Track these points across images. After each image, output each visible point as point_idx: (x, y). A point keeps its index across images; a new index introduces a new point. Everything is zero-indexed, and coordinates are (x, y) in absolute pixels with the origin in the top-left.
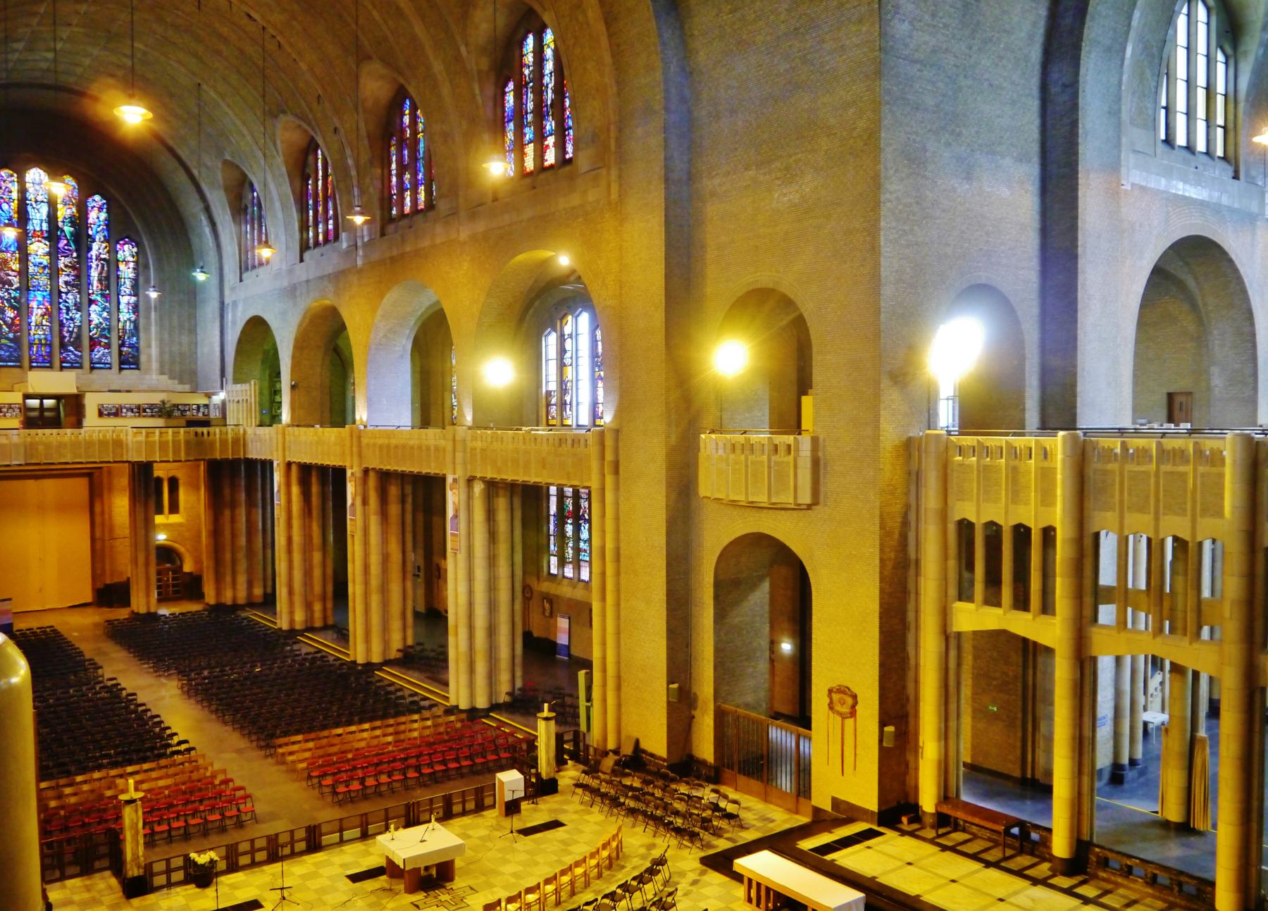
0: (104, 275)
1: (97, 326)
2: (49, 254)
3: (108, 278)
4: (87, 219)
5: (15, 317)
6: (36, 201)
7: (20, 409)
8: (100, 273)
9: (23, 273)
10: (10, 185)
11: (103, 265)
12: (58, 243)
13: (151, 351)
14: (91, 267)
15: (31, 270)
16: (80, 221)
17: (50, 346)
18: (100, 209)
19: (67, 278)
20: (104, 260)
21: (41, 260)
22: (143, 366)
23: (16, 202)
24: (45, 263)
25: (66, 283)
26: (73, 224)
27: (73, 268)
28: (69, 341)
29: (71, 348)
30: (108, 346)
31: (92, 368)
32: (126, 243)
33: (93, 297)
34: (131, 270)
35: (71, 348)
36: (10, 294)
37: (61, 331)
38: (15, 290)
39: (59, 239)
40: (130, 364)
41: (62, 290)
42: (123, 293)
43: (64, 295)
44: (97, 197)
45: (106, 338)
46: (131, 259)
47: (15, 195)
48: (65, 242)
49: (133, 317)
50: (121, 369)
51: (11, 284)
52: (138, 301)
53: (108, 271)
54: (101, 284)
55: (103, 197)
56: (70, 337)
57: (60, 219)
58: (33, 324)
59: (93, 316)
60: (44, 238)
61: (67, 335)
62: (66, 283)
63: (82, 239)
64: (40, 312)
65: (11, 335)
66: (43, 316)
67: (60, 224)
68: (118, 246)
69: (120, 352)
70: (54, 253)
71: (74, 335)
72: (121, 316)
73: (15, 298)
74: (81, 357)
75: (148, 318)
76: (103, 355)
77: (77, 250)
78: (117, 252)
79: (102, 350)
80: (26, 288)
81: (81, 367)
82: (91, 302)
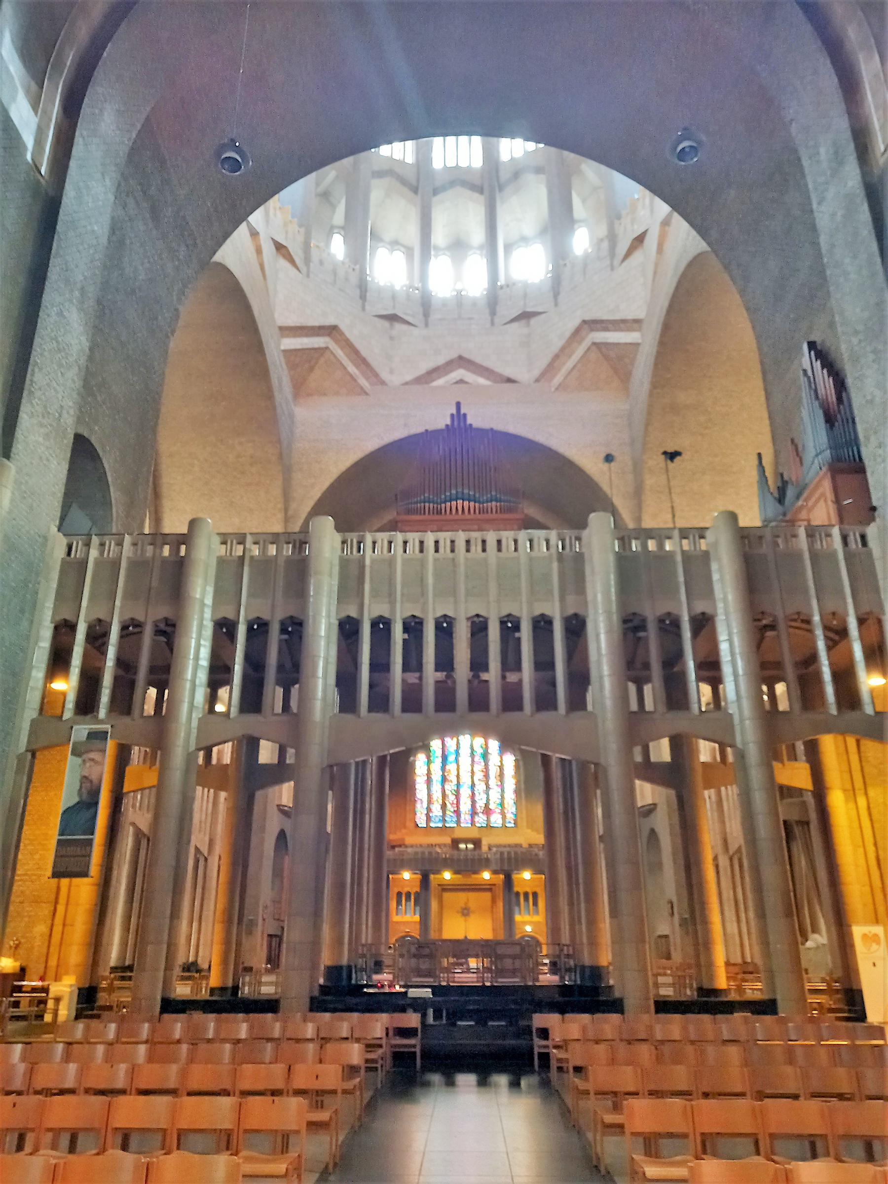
9: (458, 776)
71: (483, 808)
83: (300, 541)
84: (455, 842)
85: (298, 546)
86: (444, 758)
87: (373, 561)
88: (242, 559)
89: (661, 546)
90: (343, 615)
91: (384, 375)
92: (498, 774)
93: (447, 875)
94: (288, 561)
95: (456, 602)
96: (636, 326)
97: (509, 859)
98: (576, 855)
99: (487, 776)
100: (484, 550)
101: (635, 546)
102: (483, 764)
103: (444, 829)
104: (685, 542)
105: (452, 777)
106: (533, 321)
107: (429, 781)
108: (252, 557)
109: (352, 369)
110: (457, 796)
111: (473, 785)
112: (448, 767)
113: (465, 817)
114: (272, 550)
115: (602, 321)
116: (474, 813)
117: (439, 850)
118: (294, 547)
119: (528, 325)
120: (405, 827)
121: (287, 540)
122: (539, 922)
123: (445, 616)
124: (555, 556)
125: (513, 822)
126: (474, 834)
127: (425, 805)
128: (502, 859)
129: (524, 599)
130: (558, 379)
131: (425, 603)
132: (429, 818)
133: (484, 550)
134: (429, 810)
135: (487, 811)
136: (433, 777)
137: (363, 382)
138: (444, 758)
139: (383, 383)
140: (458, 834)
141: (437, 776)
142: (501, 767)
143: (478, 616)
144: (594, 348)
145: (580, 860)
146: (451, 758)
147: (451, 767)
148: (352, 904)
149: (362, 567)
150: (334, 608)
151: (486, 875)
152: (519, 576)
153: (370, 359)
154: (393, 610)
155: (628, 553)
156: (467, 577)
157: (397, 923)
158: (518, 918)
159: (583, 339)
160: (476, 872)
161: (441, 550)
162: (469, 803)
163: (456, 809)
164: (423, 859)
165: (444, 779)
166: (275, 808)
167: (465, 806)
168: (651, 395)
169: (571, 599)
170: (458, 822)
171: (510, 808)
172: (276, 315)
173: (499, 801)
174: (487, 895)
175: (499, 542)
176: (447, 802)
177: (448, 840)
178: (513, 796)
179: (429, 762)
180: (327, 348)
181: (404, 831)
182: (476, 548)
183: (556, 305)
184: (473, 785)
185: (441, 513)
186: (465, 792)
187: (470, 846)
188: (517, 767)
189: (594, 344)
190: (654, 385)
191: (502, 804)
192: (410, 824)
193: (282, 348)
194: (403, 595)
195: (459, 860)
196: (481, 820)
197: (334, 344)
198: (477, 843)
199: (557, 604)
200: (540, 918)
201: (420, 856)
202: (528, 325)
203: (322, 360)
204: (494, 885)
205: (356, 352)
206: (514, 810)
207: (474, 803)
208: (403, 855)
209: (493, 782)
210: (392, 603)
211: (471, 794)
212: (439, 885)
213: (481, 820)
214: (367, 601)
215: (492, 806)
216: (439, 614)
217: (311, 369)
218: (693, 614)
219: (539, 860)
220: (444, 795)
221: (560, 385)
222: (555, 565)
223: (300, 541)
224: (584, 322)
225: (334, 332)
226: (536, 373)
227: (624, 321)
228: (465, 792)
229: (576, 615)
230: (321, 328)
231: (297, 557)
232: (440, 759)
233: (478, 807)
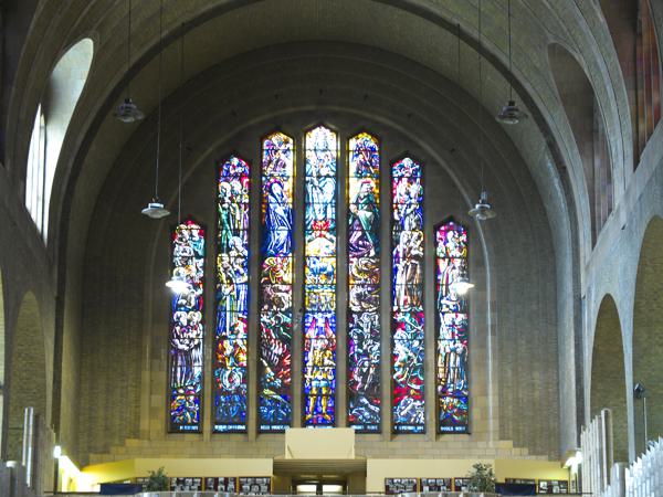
0: (416, 281)
1: (405, 364)
2: (335, 254)
3: (421, 286)
4: (393, 195)
5: (285, 354)
6: (319, 177)
7: (268, 485)
8: (412, 279)
9: (299, 286)
10: (283, 157)
11: (414, 266)
12: (349, 237)
13: (488, 403)
14: (396, 269)
15: (308, 281)
16: (382, 203)
17: (333, 397)
18: (411, 180)
19: (360, 290)
21: (325, 265)
22: (475, 428)
23: (291, 180)
24: (330, 269)
25: (359, 297)
26: (371, 205)
27: (371, 273)
28: (361, 389)
29: (365, 400)
30: (420, 396)
31: (395, 433)
32: (451, 229)
33: (400, 317)
34: (457, 271)
35: (365, 400)
36: (279, 319)
37: (349, 375)
38: (286, 313)
39: (350, 231)
40: (455, 423)
41: (354, 309)
42: (445, 309)
44: (407, 162)
45: (418, 382)
46: (458, 254)
47: (289, 171)
48: (360, 234)
49: (460, 347)
50: (439, 433)
51: (280, 304)
52: (467, 321)
53: (423, 274)
54: (411, 296)
55: (415, 160)
56: (364, 382)
57: (353, 199)
58: (310, 364)
59: (400, 349)
60: (328, 230)
61: (359, 379)
62: (359, 297)
63: (384, 227)
64: (320, 344)
65: (278, 382)
66: (324, 350)
67: (353, 208)
68: (438, 235)
69: (439, 408)
70: (345, 251)
71: (369, 380)
72: (441, 345)
73: (285, 325)
74: (380, 413)
75: (483, 346)
76: (413, 410)
77: (376, 245)
78: (436, 244)
79: (412, 403)
81: (378, 432)
82: (395, 326)
86: (260, 231)
120: (136, 434)
138: (260, 231)
141: (235, 292)
165: (259, 298)
177: (263, 467)
179: (215, 247)
181: (133, 443)
220: (258, 342)
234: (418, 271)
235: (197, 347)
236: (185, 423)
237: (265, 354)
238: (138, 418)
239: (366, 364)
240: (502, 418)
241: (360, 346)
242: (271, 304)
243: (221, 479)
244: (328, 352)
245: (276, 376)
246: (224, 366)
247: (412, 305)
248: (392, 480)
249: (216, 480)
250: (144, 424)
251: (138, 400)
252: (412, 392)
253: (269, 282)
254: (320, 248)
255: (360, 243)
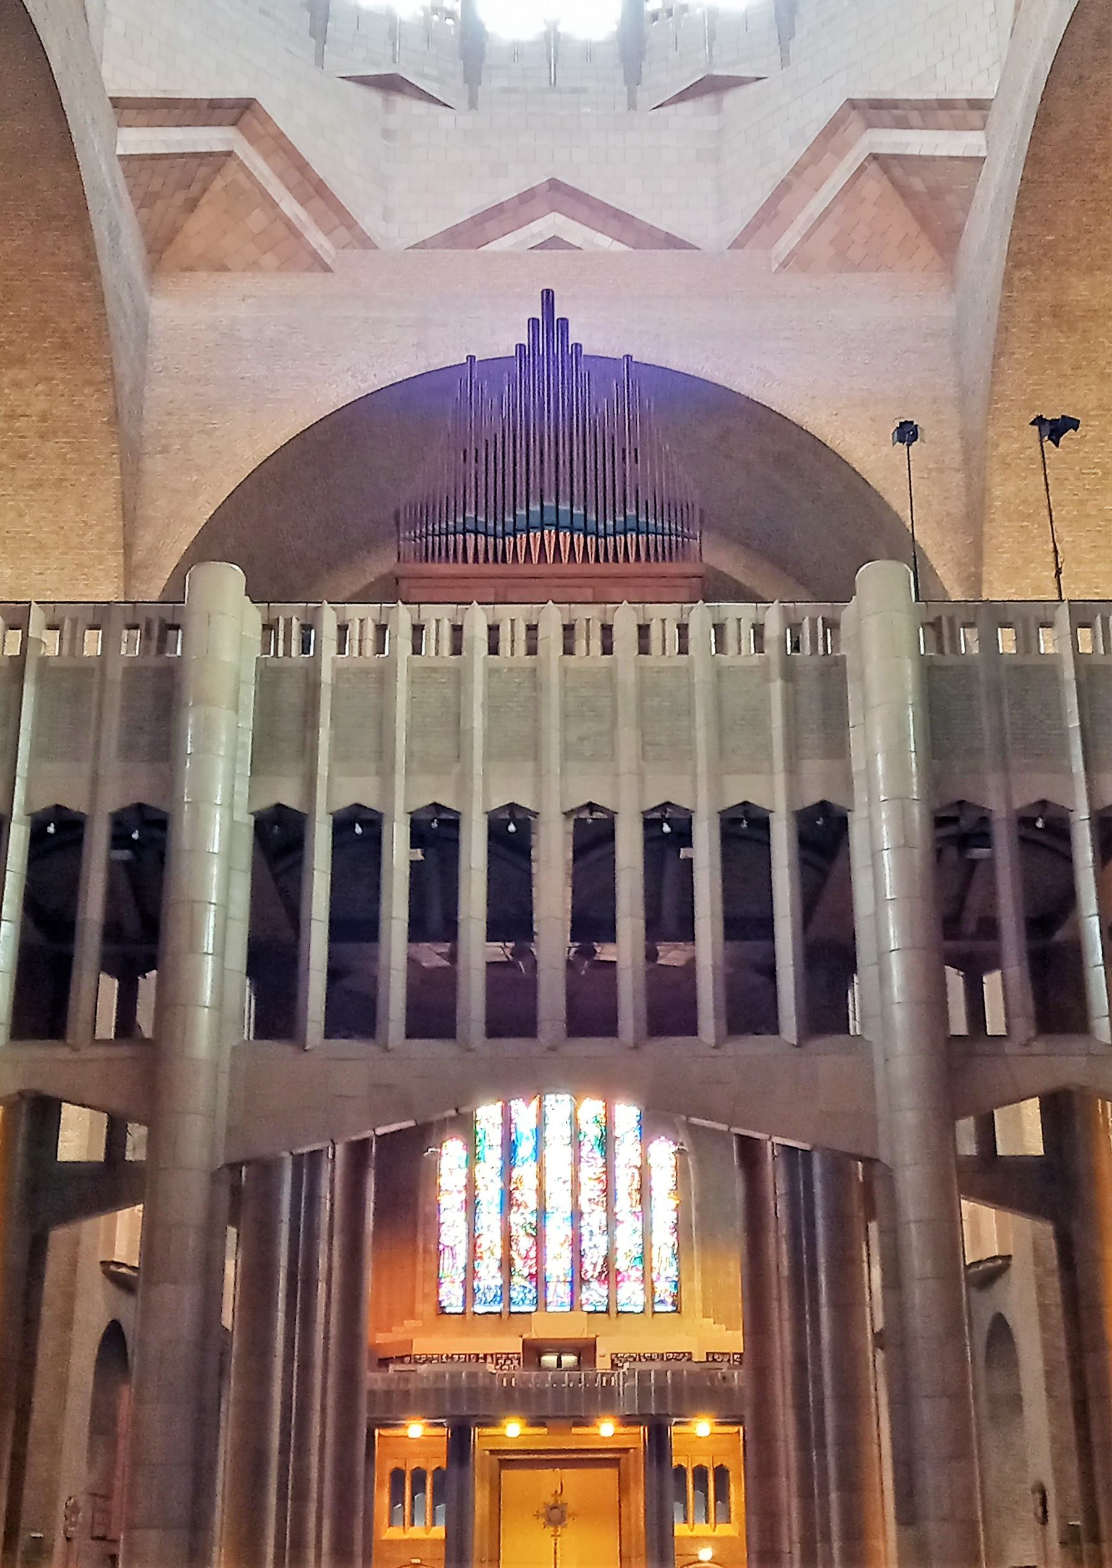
7: (519, 1359)
9: (541, 1192)
20: (636, 1167)
28: (592, 1276)
43: (585, 1216)
51: (526, 1207)
56: (594, 1270)
70: (577, 1160)
71: (599, 1269)
73: (530, 1224)
80: (542, 1212)
83: (162, 621)
84: (533, 1351)
85: (155, 633)
86: (509, 1147)
87: (339, 673)
88: (18, 665)
89: (1027, 642)
90: (266, 802)
91: (369, 223)
92: (636, 1185)
93: (513, 1429)
94: (133, 671)
95: (538, 774)
96: (975, 116)
97: (661, 1390)
98: (818, 1379)
99: (609, 1192)
100: (607, 650)
101: (969, 641)
102: (601, 1161)
103: (506, 1318)
104: (1084, 634)
105: (526, 1195)
106: (731, 99)
107: (471, 1204)
108: (44, 660)
109: (290, 207)
110: (539, 1236)
111: (577, 1215)
112: (515, 1173)
113: (558, 1294)
114: (92, 643)
115: (894, 104)
116: (577, 1281)
117: (491, 1367)
118: (147, 635)
119: (718, 109)
120: (412, 1315)
121: (130, 622)
122: (730, 1539)
123: (512, 807)
124: (775, 669)
125: (669, 1300)
126: (577, 1329)
127: (462, 1260)
128: (643, 1391)
129: (702, 766)
130: (788, 241)
131: (464, 780)
132: (470, 1293)
133: (607, 650)
134: (471, 1272)
135: (609, 1274)
136: (483, 1195)
137: (317, 239)
138: (509, 1147)
139: (365, 242)
140: (540, 1330)
142: (644, 1171)
143: (591, 807)
144: (873, 167)
145: (828, 1391)
146: (525, 1149)
147: (526, 1172)
148: (282, 1497)
149: (313, 687)
150: (242, 787)
151: (607, 1428)
152: (690, 712)
153: (332, 184)
154: (387, 790)
155: (949, 659)
156: (565, 716)
157: (391, 1542)
158: (680, 1529)
159: (848, 146)
160: (582, 1421)
161: (505, 646)
162: (567, 1254)
163: (533, 1271)
164: (455, 1392)
165: (508, 1201)
166: (99, 1267)
167: (558, 1266)
168: (1007, 282)
169: (813, 768)
170: (540, 1301)
171: (665, 1268)
172: (106, 71)
173: (637, 1251)
174: (611, 1473)
175: (643, 630)
176: (514, 1254)
178: (672, 1239)
179: (473, 1158)
180: (230, 154)
182: (589, 645)
183: (785, 61)
184: (577, 1215)
185: (504, 561)
186: (558, 1231)
187: (569, 1360)
188: (681, 1171)
189: (875, 157)
190: (1016, 259)
191: (644, 1258)
192: (425, 1308)
193: (120, 151)
194: (410, 755)
195: (542, 1392)
196: (594, 1295)
197: (245, 144)
198: (585, 1351)
199: (780, 780)
200: (732, 1530)
201: (447, 1385)
202: (718, 109)
203: (218, 184)
204: (626, 1450)
205: (302, 166)
206: (672, 1272)
207: (578, 1256)
208: (407, 1380)
209: (625, 1204)
210: (386, 773)
211: (569, 1232)
212: (492, 1452)
213: (594, 1295)
214: (323, 769)
215: (621, 1264)
216: (497, 802)
217: (192, 205)
218: (1099, 806)
219: (730, 1390)
220: (508, 1240)
221: (792, 254)
222: (776, 688)
223: (162, 621)
224: (852, 104)
225: (248, 116)
226: (737, 224)
227: (946, 105)
228: (558, 1231)
229: (824, 807)
230: (214, 105)
231: (153, 661)
232: (497, 1152)
233: (587, 1265)
234: (637, 1178)
235: (460, 1242)
236: (451, 1305)
237: (514, 1247)
238: (413, 1303)
239: (596, 1255)
240: (705, 1300)
241: (590, 1240)
242: (519, 1206)
243: (481, 1355)
244: (566, 1245)
245: (524, 1266)
246: (481, 1258)
247: (631, 1206)
248: (617, 1354)
249: (477, 1355)
250: (419, 1308)
251: (414, 1287)
252: (632, 1278)
253: (517, 1188)
254: (558, 1156)
255: (591, 1155)
